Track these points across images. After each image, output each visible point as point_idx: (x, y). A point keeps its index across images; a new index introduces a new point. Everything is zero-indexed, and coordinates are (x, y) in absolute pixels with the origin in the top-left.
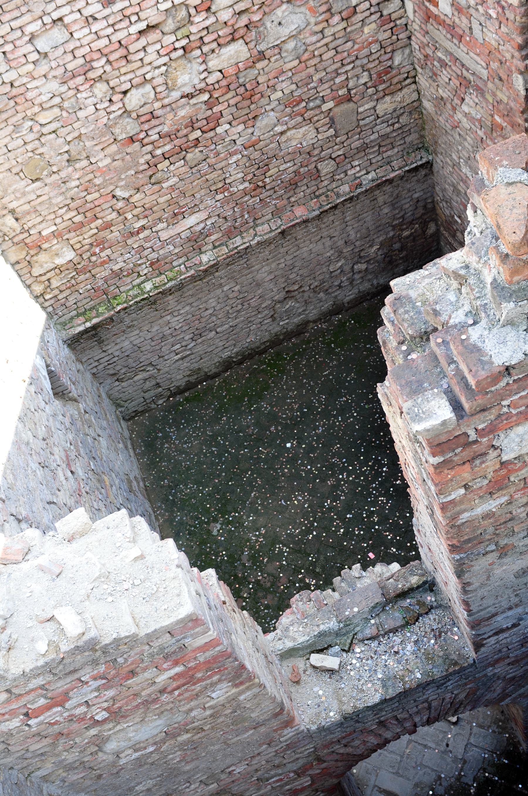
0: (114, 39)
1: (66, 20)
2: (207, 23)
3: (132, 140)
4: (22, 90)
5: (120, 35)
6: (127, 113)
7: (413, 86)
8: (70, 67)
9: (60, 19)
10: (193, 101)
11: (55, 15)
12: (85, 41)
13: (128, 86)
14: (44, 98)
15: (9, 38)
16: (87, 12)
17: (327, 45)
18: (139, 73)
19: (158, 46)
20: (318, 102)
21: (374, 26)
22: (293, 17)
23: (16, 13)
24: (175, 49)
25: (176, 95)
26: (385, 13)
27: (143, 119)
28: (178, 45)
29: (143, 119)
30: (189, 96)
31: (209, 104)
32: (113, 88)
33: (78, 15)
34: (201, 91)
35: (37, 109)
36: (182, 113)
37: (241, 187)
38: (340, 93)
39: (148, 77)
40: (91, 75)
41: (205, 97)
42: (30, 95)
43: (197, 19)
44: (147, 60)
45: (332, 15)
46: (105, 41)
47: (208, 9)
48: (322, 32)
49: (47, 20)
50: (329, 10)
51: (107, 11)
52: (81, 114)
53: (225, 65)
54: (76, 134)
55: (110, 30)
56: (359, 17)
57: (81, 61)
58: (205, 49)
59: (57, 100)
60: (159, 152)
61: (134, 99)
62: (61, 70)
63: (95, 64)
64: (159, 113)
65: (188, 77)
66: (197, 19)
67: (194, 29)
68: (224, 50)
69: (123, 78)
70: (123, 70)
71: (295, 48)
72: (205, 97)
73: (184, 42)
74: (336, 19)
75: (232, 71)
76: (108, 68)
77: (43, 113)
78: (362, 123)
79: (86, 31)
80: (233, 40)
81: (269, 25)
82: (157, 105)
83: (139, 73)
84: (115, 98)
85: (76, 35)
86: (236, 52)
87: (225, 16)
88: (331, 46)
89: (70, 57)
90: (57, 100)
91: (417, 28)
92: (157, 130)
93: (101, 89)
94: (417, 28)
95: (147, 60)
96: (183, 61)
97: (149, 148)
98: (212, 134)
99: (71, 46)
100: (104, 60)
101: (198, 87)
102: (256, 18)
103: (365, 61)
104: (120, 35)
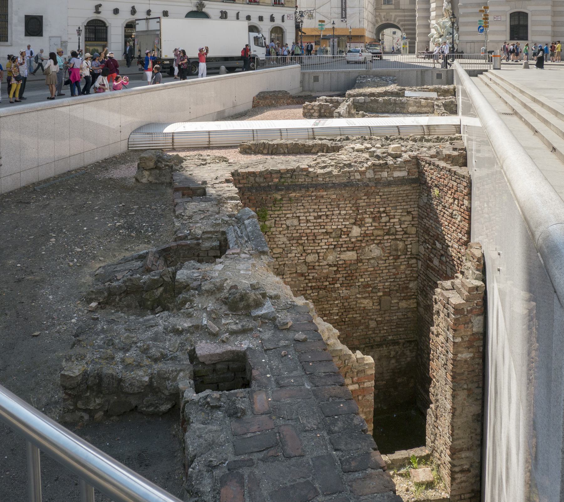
0: (313, 231)
2: (346, 239)
3: (302, 275)
4: (273, 236)
5: (316, 231)
6: (305, 262)
7: (415, 300)
8: (294, 235)
9: (299, 217)
10: (330, 268)
11: (298, 215)
12: (303, 228)
13: (310, 251)
14: (280, 243)
15: (280, 216)
16: (308, 218)
17: (386, 267)
18: (316, 248)
19: (326, 241)
20: (377, 290)
21: (404, 267)
22: (376, 250)
24: (332, 245)
25: (325, 263)
26: (410, 263)
27: (310, 267)
28: (333, 243)
29: (310, 267)
30: (330, 266)
31: (336, 272)
32: (304, 250)
33: (304, 218)
34: (335, 265)
35: (275, 246)
36: (325, 271)
37: (335, 318)
38: (386, 290)
39: (319, 251)
40: (300, 241)
41: (335, 269)
42: (276, 239)
43: (343, 236)
44: (321, 244)
45: (391, 256)
46: (309, 231)
47: (348, 235)
48: (385, 260)
49: (295, 215)
50: (389, 253)
51: (315, 221)
52: (289, 255)
53: (347, 259)
54: (283, 262)
55: (313, 228)
57: (298, 235)
58: (342, 249)
59: (284, 246)
60: (310, 285)
61: (310, 258)
62: (291, 235)
63: (303, 238)
64: (317, 267)
65: (331, 258)
66: (343, 236)
67: (341, 240)
68: (348, 253)
69: (309, 248)
70: (311, 245)
71: (374, 263)
72: (335, 269)
73: (336, 243)
74: (391, 258)
75: (348, 262)
76: (306, 241)
77: (277, 249)
78: (392, 308)
79: (305, 224)
80: (353, 250)
81: (367, 249)
82: (317, 264)
83: (316, 248)
84: (304, 254)
85: (301, 225)
86: (351, 255)
87: (353, 240)
88: (388, 268)
89: (295, 231)
90: (284, 246)
91: (422, 272)
92: (313, 275)
93: (301, 247)
94: (422, 272)
95: (321, 244)
96: (332, 250)
97: (307, 281)
98: (332, 286)
99: (298, 228)
100: (306, 238)
101: (334, 263)
102: (363, 245)
103: (398, 280)
104: (316, 231)
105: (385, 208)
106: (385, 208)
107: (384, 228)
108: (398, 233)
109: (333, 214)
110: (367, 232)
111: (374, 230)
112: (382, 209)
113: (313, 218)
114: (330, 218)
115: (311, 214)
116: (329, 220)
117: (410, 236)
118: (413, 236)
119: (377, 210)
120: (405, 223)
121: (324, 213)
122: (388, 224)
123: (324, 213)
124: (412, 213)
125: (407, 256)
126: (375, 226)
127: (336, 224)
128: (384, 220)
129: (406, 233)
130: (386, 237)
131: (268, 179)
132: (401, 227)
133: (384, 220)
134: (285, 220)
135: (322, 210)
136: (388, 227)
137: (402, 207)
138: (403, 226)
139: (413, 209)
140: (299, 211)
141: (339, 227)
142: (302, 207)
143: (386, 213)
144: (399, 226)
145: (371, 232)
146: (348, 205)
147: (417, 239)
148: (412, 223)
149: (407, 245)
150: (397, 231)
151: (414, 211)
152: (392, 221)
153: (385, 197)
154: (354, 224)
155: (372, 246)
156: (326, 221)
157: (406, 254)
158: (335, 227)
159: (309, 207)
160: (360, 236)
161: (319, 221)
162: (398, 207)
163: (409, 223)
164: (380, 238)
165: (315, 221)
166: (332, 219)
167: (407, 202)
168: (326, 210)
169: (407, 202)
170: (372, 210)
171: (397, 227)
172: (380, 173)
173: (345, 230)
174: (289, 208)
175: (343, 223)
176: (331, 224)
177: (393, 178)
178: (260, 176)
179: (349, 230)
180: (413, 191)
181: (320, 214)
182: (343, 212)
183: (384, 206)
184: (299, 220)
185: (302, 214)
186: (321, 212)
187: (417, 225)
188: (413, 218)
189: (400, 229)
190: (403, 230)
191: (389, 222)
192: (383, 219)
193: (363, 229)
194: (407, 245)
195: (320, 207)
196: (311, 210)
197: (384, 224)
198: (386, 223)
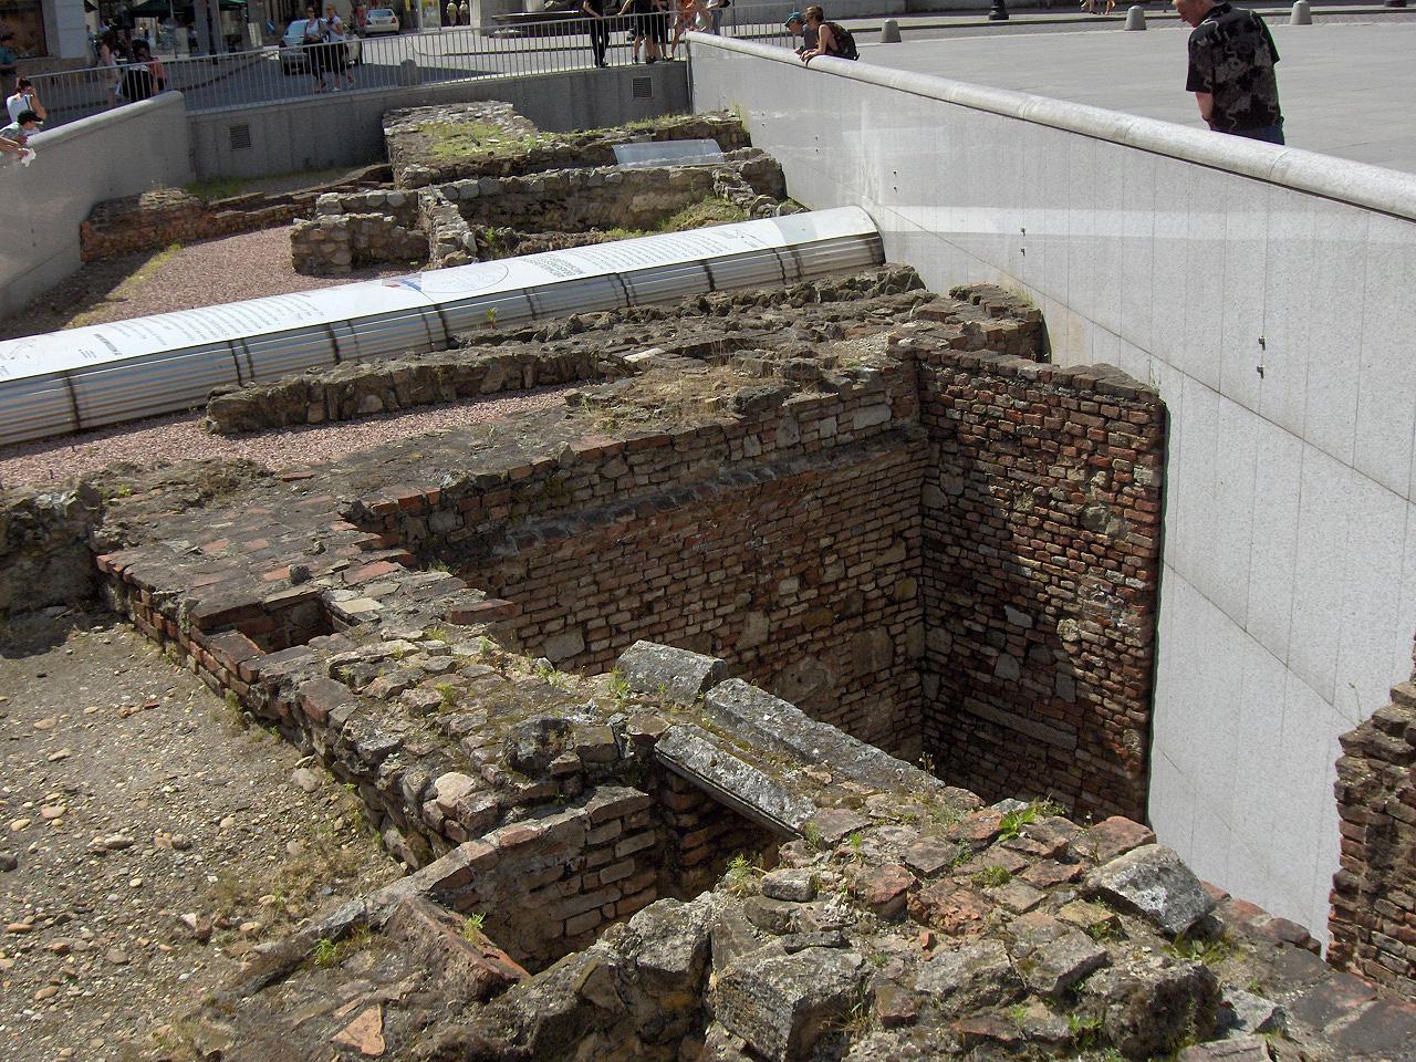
1: (591, 625)
9: (584, 623)
11: (581, 617)
16: (614, 620)
23: (543, 604)
47: (733, 646)
49: (571, 620)
51: (635, 624)
56: (879, 687)
74: (857, 685)
79: (605, 643)
85: (594, 647)
105: (834, 535)
106: (834, 535)
107: (835, 599)
108: (873, 606)
109: (687, 590)
110: (787, 625)
111: (804, 612)
112: (825, 542)
113: (628, 616)
114: (677, 602)
115: (622, 605)
116: (676, 612)
117: (903, 607)
118: (912, 604)
119: (812, 546)
120: (889, 571)
121: (661, 593)
122: (842, 585)
123: (661, 593)
124: (907, 534)
125: (895, 670)
126: (808, 601)
127: (699, 618)
128: (831, 574)
129: (891, 601)
130: (838, 628)
131: (473, 515)
132: (877, 587)
133: (831, 574)
134: (541, 644)
135: (655, 584)
136: (843, 595)
137: (878, 524)
138: (883, 581)
139: (907, 523)
140: (582, 603)
141: (708, 626)
142: (593, 588)
143: (837, 552)
144: (873, 585)
145: (798, 620)
146: (731, 551)
147: (920, 611)
148: (908, 565)
149: (893, 637)
150: (866, 601)
151: (911, 527)
152: (852, 572)
153: (834, 499)
154: (751, 606)
155: (802, 666)
156: (667, 616)
157: (894, 665)
158: (696, 629)
159: (613, 583)
160: (769, 642)
161: (648, 620)
162: (869, 527)
163: (898, 568)
164: (822, 634)
165: (635, 624)
166: (684, 605)
167: (890, 505)
168: (666, 580)
169: (890, 505)
170: (797, 550)
171: (867, 588)
172: (817, 424)
173: (724, 632)
174: (553, 600)
175: (720, 612)
176: (682, 622)
177: (852, 431)
178: (444, 508)
179: (735, 628)
180: (911, 466)
181: (648, 597)
182: (717, 575)
183: (833, 528)
184: (586, 634)
185: (595, 612)
186: (650, 590)
187: (918, 571)
188: (908, 550)
189: (877, 593)
190: (884, 595)
191: (846, 577)
192: (830, 570)
193: (774, 617)
194: (893, 637)
195: (650, 574)
196: (621, 592)
197: (832, 588)
198: (836, 583)
